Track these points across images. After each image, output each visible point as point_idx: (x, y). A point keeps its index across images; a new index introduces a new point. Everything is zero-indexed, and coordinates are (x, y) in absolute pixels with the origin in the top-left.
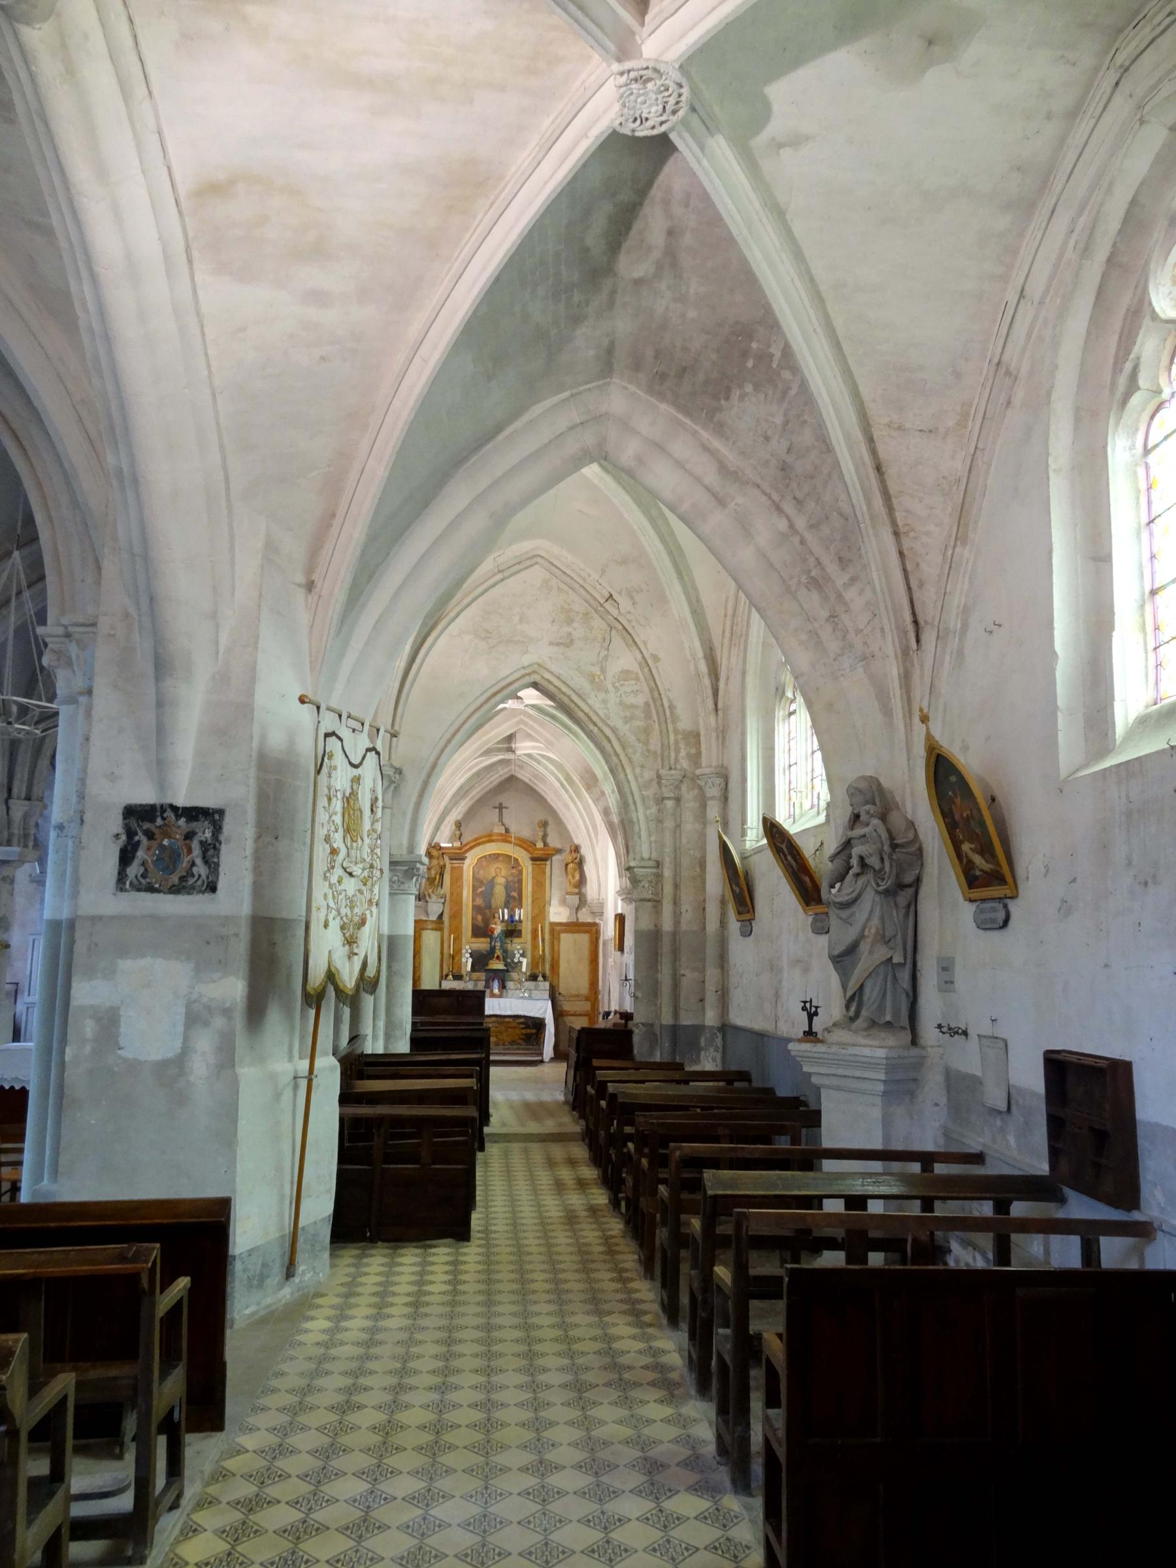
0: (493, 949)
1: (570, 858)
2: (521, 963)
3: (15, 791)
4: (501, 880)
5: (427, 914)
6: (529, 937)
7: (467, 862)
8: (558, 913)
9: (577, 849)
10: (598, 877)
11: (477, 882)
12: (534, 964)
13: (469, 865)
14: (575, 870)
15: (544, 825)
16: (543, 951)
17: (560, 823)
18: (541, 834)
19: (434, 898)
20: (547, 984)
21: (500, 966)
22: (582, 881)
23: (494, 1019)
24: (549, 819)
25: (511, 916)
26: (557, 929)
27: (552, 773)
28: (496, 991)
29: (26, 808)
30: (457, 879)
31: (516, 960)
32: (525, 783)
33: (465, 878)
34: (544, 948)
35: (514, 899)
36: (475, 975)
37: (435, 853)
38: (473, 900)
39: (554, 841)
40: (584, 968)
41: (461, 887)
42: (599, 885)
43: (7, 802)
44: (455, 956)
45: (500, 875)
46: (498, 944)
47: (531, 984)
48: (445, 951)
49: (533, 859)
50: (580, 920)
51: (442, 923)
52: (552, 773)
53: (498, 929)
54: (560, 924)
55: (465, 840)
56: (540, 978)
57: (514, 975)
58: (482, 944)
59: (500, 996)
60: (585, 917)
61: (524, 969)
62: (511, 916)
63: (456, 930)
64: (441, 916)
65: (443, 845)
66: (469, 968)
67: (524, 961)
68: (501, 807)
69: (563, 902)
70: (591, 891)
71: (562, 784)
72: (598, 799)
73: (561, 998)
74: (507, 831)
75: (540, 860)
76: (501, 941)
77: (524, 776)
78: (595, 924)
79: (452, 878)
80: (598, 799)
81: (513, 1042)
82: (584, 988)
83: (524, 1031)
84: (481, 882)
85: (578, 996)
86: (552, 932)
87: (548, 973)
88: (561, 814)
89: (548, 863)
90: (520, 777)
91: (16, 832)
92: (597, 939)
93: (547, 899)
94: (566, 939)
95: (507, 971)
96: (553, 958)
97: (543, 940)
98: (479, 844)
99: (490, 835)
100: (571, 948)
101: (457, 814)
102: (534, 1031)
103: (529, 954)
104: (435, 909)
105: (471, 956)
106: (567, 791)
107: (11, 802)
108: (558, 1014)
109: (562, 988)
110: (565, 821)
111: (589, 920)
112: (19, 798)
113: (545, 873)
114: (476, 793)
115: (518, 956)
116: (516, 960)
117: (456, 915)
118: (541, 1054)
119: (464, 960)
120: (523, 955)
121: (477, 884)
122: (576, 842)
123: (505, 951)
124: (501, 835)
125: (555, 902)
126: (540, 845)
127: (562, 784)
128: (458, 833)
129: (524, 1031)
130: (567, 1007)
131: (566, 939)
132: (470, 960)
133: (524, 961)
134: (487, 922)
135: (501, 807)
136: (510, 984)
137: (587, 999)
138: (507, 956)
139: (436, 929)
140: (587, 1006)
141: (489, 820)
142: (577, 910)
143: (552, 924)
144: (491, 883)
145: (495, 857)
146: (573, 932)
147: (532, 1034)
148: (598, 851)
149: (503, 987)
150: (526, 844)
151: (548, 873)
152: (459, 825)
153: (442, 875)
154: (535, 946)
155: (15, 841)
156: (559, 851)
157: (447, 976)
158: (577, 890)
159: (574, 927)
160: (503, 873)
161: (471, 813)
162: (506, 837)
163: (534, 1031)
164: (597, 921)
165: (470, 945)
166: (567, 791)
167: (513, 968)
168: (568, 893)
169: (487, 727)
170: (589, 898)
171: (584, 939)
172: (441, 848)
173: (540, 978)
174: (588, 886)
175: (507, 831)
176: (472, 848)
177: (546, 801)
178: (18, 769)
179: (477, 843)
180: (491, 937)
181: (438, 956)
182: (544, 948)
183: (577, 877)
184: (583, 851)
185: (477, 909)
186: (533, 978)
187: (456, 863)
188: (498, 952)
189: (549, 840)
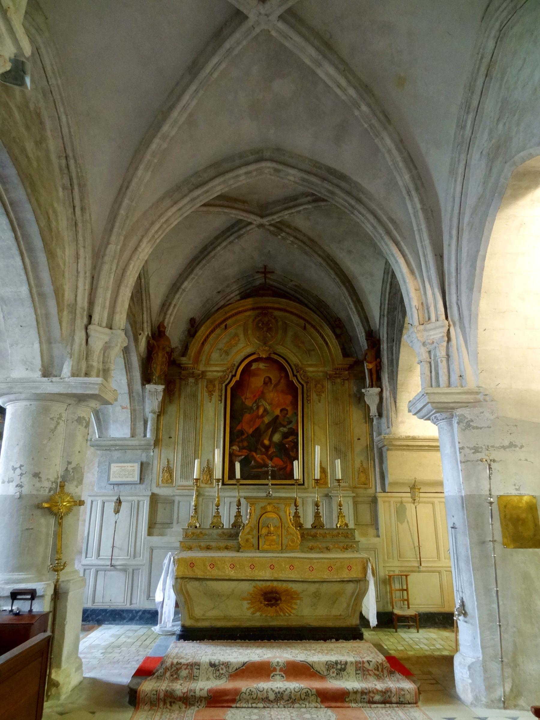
3: (96, 318)
29: (107, 339)
43: (86, 329)
91: (95, 364)
107: (91, 327)
112: (100, 325)
155: (94, 373)
178: (100, 292)
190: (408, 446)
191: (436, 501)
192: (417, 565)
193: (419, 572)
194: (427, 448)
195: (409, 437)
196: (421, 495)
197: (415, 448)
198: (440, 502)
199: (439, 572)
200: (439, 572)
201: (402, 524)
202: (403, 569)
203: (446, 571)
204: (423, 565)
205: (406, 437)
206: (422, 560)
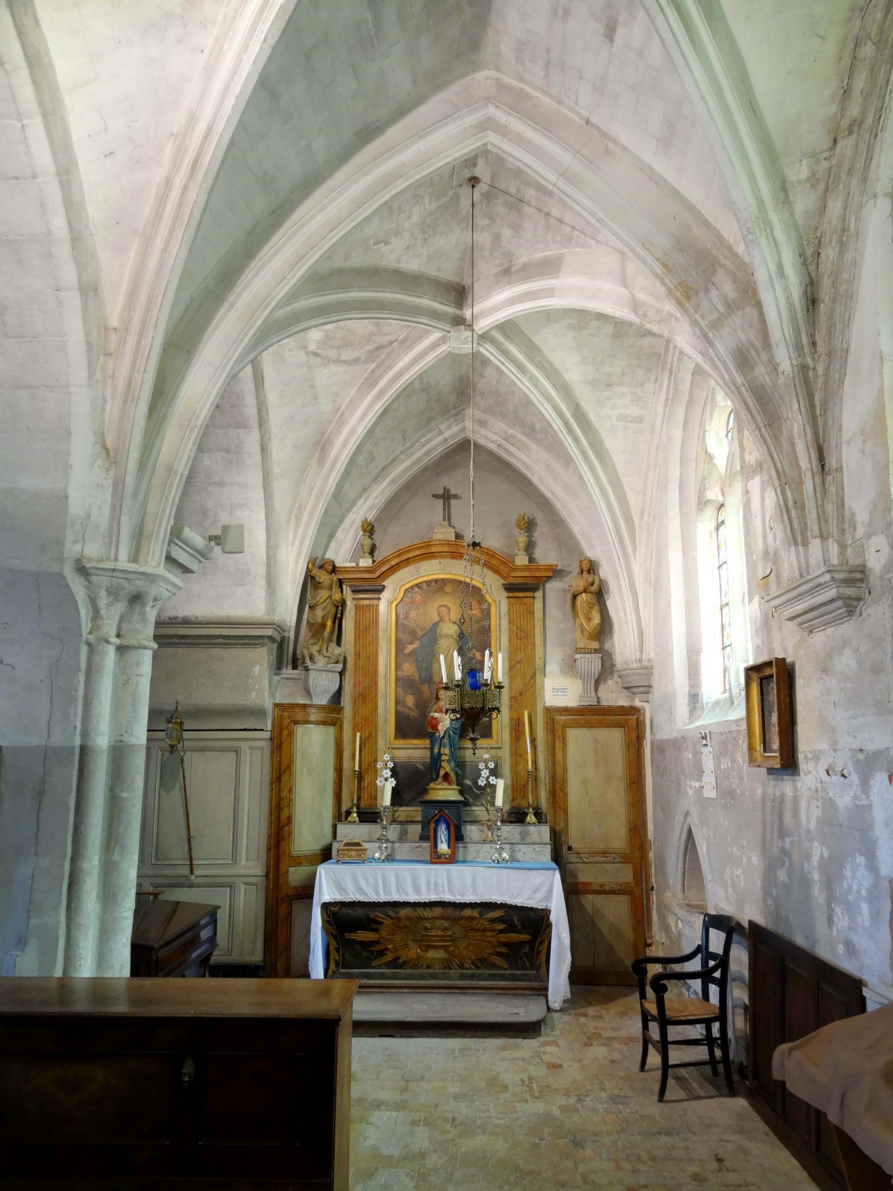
0: (436, 761)
1: (580, 584)
2: (493, 787)
4: (450, 629)
5: (308, 693)
6: (506, 735)
7: (385, 595)
8: (559, 690)
9: (591, 568)
10: (639, 619)
11: (405, 632)
12: (517, 790)
13: (386, 606)
14: (591, 606)
15: (529, 526)
16: (535, 762)
17: (557, 521)
18: (522, 539)
19: (321, 662)
20: (544, 832)
21: (447, 793)
22: (604, 629)
23: (438, 911)
24: (536, 515)
25: (472, 671)
26: (559, 720)
27: (549, 399)
28: (443, 847)
30: (368, 626)
31: (482, 782)
32: (491, 453)
33: (382, 624)
34: (536, 758)
35: (474, 641)
36: (404, 812)
37: (323, 577)
38: (397, 668)
39: (546, 555)
40: (616, 797)
41: (375, 642)
42: (641, 633)
44: (364, 775)
45: (446, 616)
46: (446, 751)
47: (510, 831)
48: (346, 764)
49: (510, 588)
50: (605, 703)
51: (340, 710)
52: (549, 399)
53: (445, 722)
54: (566, 710)
55: (379, 555)
56: (531, 818)
57: (479, 811)
58: (415, 751)
59: (451, 859)
60: (612, 695)
61: (499, 801)
62: (472, 671)
63: (367, 725)
64: (338, 695)
65: (338, 564)
66: (387, 800)
67: (500, 785)
68: (446, 497)
69: (570, 667)
70: (624, 645)
71: (567, 424)
72: (715, 325)
73: (573, 858)
74: (458, 536)
75: (524, 587)
76: (452, 745)
77: (491, 436)
78: (634, 710)
79: (357, 627)
80: (715, 325)
81: (482, 962)
82: (619, 840)
83: (503, 938)
84: (413, 634)
85: (605, 853)
86: (551, 726)
87: (544, 804)
88: (559, 506)
89: (539, 594)
90: (482, 442)
92: (640, 738)
93: (538, 662)
94: (578, 740)
95: (466, 803)
96: (553, 778)
97: (533, 741)
98: (407, 562)
99: (428, 545)
100: (588, 758)
101: (366, 508)
102: (524, 937)
103: (506, 770)
104: (322, 683)
105: (395, 773)
106: (576, 440)
108: (573, 891)
109: (574, 838)
110: (564, 514)
111: (623, 702)
113: (531, 613)
114: (402, 470)
115: (485, 773)
116: (482, 782)
117: (367, 697)
118: (542, 991)
119: (379, 782)
120: (495, 772)
121: (404, 637)
122: (589, 554)
123: (461, 765)
124: (448, 543)
125: (553, 667)
126: (522, 560)
127: (567, 424)
128: (367, 542)
129: (503, 938)
130: (586, 875)
131: (578, 740)
132: (392, 783)
133: (500, 785)
134: (423, 706)
135: (446, 497)
136: (472, 831)
137: (626, 859)
138: (463, 775)
139: (324, 723)
140: (625, 875)
141: (426, 520)
142: (597, 682)
143: (550, 711)
144: (432, 636)
145: (438, 586)
146: (591, 726)
147: (522, 943)
148: (636, 566)
149: (457, 837)
150: (494, 562)
151: (538, 613)
152: (369, 529)
153: (338, 620)
154: (517, 754)
156: (556, 573)
157: (348, 813)
158: (595, 645)
159: (593, 715)
160: (455, 614)
161: (392, 507)
162: (455, 549)
163: (524, 937)
164: (637, 703)
165: (392, 752)
166: (576, 440)
167: (477, 797)
168: (578, 650)
169: (393, 133)
170: (619, 660)
171: (614, 738)
172: (334, 570)
173: (531, 818)
174: (616, 637)
175: (458, 536)
176: (393, 569)
177: (530, 483)
179: (403, 560)
180: (432, 736)
181: (330, 775)
182: (536, 758)
183: (596, 619)
184: (605, 572)
185: (404, 683)
186: (517, 816)
187: (366, 599)
188: (447, 767)
189: (538, 553)
190: (183, 637)
191: (244, 746)
192: (186, 871)
193: (191, 886)
194: (221, 640)
195: (176, 618)
196: (186, 735)
197: (196, 641)
198: (252, 748)
199: (231, 886)
200: (231, 887)
201: (168, 793)
202: (158, 880)
203: (246, 884)
204: (196, 872)
205: (170, 618)
206: (194, 862)
